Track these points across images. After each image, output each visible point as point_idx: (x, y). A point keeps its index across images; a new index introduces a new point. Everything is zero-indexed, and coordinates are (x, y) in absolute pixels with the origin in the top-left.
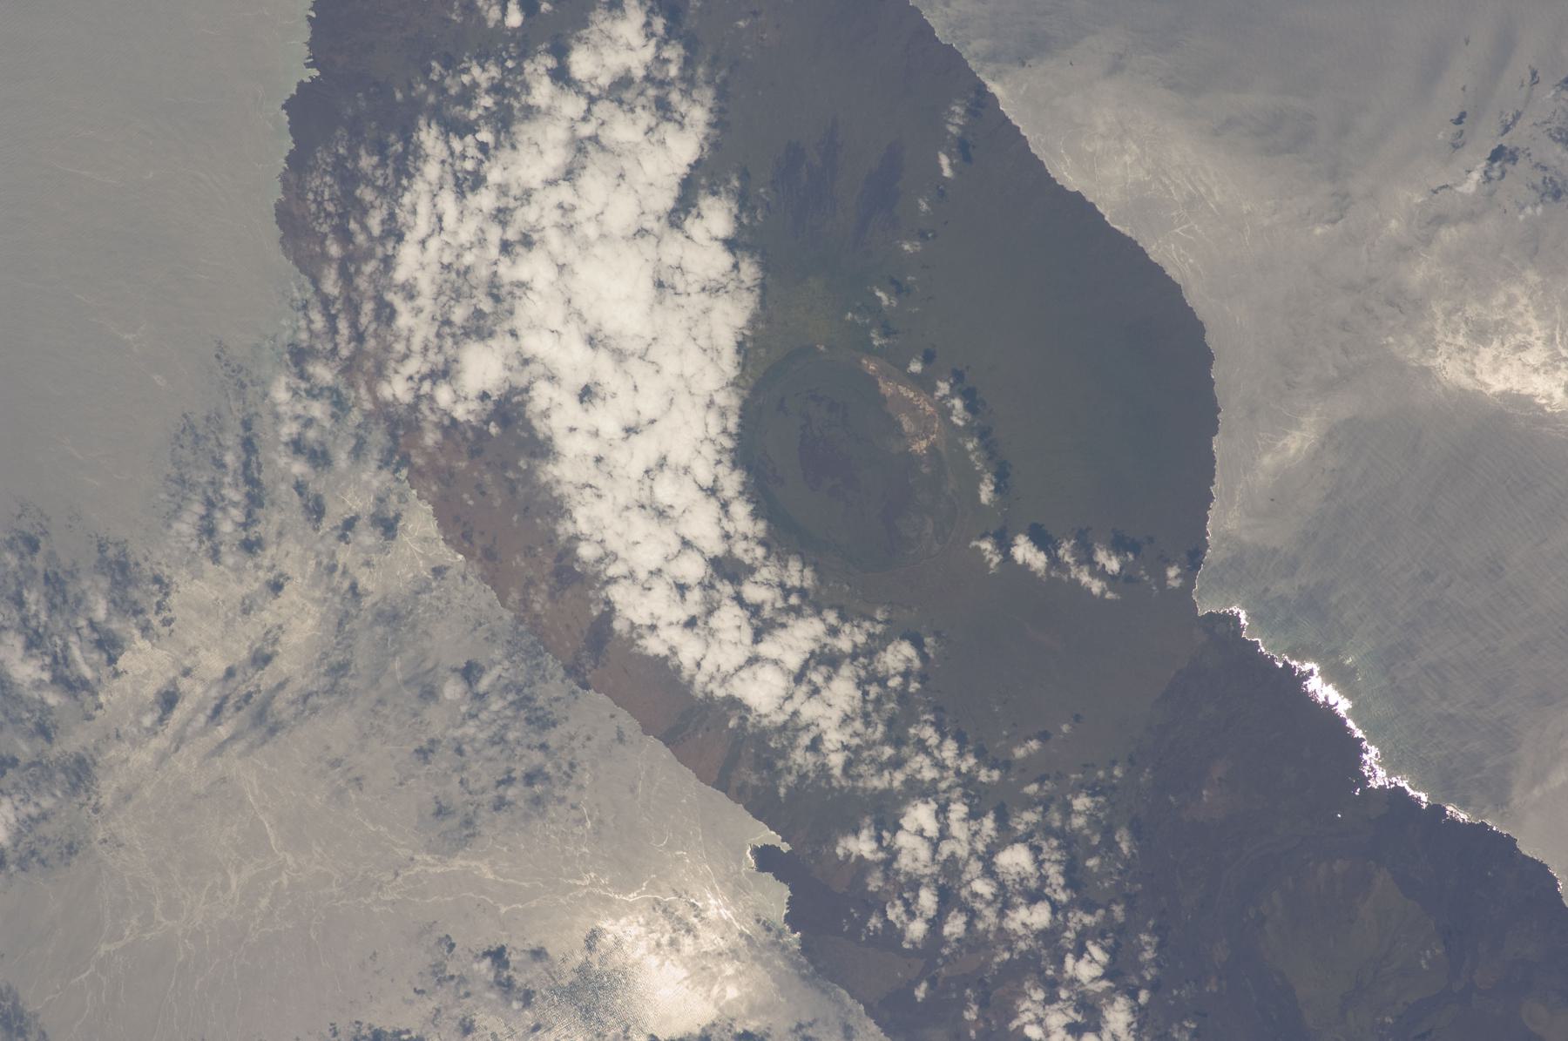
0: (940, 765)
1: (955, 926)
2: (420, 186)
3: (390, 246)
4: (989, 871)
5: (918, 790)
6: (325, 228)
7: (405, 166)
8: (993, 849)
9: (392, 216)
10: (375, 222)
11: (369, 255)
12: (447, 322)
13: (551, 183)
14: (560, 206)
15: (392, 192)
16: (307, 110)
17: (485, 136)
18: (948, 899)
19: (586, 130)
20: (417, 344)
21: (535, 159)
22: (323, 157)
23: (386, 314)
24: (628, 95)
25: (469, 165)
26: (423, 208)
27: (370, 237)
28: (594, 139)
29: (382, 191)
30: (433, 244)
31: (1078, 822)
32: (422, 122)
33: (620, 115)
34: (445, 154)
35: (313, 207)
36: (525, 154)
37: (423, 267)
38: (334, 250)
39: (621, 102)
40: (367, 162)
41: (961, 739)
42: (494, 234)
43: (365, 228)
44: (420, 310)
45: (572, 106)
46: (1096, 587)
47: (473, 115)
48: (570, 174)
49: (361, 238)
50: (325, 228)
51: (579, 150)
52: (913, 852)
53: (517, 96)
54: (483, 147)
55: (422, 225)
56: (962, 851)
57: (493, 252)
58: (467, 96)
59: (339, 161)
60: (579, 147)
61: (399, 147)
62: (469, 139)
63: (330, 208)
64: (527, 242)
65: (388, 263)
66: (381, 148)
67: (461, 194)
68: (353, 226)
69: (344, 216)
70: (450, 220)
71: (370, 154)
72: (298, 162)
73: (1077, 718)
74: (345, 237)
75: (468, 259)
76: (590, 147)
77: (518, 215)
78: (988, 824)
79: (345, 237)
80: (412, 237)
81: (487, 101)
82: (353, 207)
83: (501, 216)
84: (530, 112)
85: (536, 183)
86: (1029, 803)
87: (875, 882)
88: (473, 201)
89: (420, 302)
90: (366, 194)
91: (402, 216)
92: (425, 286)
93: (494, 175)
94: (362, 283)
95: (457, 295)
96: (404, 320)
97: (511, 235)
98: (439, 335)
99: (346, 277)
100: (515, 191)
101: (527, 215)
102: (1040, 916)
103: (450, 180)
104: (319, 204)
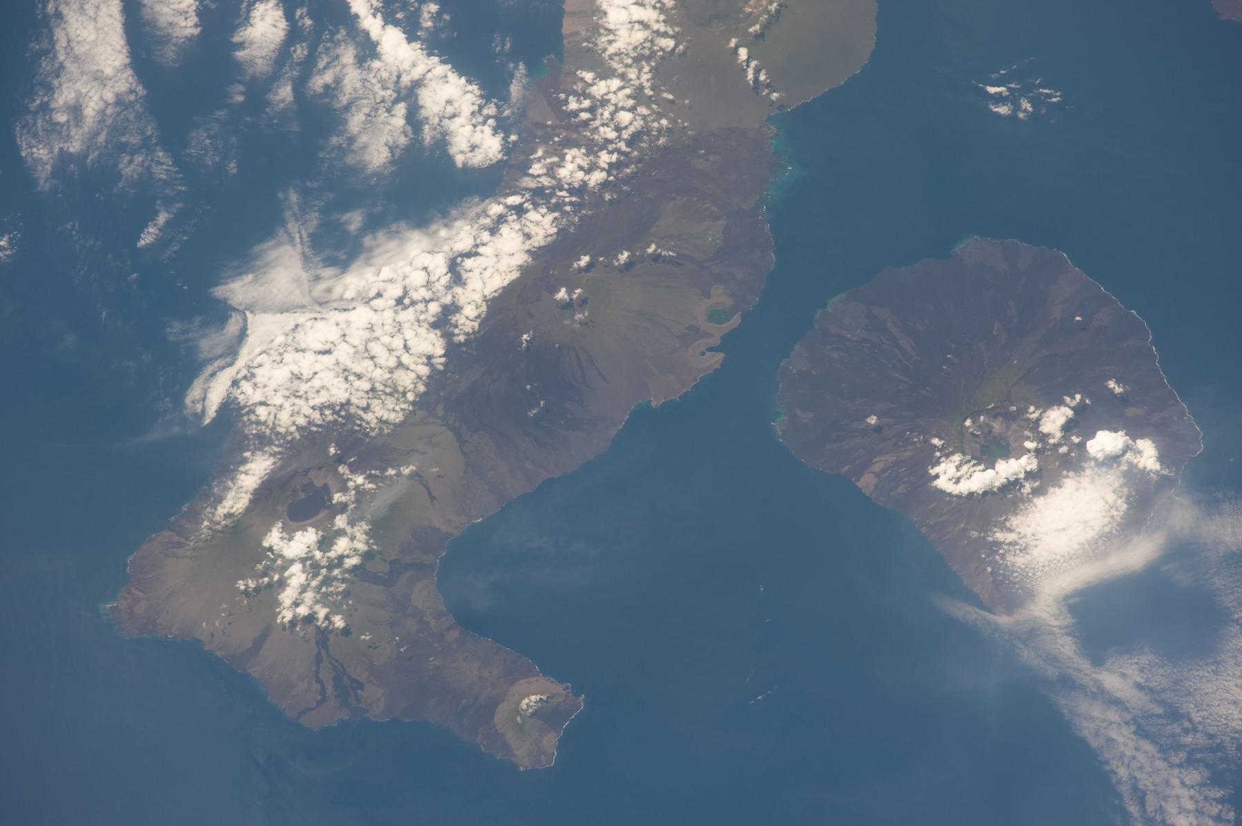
0: (638, 78)
1: (585, 116)
4: (613, 114)
5: (623, 77)
8: (623, 108)
18: (592, 110)
31: (655, 125)
41: (652, 78)
46: (750, 76)
52: (600, 89)
56: (613, 102)
73: (691, 108)
78: (631, 102)
86: (648, 107)
87: (579, 87)
102: (612, 135)
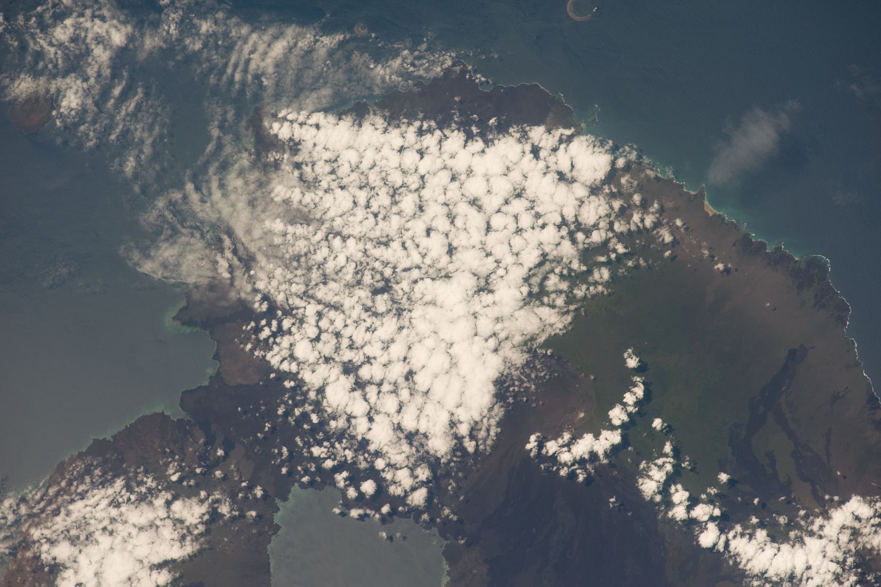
2: (103, 492)
3: (78, 497)
6: (68, 477)
7: (104, 483)
9: (87, 491)
10: (81, 488)
11: (70, 495)
12: (68, 531)
13: (135, 526)
14: (130, 534)
15: (94, 485)
16: (99, 448)
17: (133, 497)
19: (158, 522)
20: (54, 528)
21: (138, 516)
22: (88, 460)
23: (56, 512)
24: (178, 525)
25: (120, 500)
26: (97, 498)
27: (75, 491)
28: (157, 527)
29: (92, 482)
30: (89, 509)
32: (122, 478)
33: (170, 528)
34: (118, 491)
35: (71, 469)
36: (137, 512)
37: (79, 511)
38: (63, 484)
39: (175, 525)
40: (97, 472)
42: (106, 523)
43: (77, 487)
44: (66, 521)
45: (162, 513)
47: (136, 489)
48: (141, 529)
49: (73, 488)
50: (68, 477)
51: (151, 526)
53: (152, 496)
54: (129, 499)
55: (92, 501)
57: (100, 526)
58: (140, 483)
59: (92, 465)
60: (152, 525)
61: (109, 477)
62: (128, 494)
63: (75, 473)
64: (111, 533)
65: (72, 501)
66: (104, 473)
67: (109, 505)
68: (75, 483)
69: (76, 479)
70: (99, 508)
71: (101, 471)
72: (81, 456)
74: (70, 484)
75: (92, 521)
76: (154, 528)
77: (117, 525)
79: (70, 484)
80: (85, 501)
81: (143, 490)
82: (81, 478)
83: (113, 520)
84: (151, 503)
85: (131, 522)
88: (111, 509)
89: (68, 519)
90: (88, 479)
91: (89, 494)
92: (74, 517)
93: (123, 508)
94: (60, 499)
95: (78, 527)
96: (58, 519)
97: (110, 528)
98: (62, 532)
99: (57, 494)
100: (123, 518)
101: (119, 527)
103: (111, 498)
104: (74, 469)
